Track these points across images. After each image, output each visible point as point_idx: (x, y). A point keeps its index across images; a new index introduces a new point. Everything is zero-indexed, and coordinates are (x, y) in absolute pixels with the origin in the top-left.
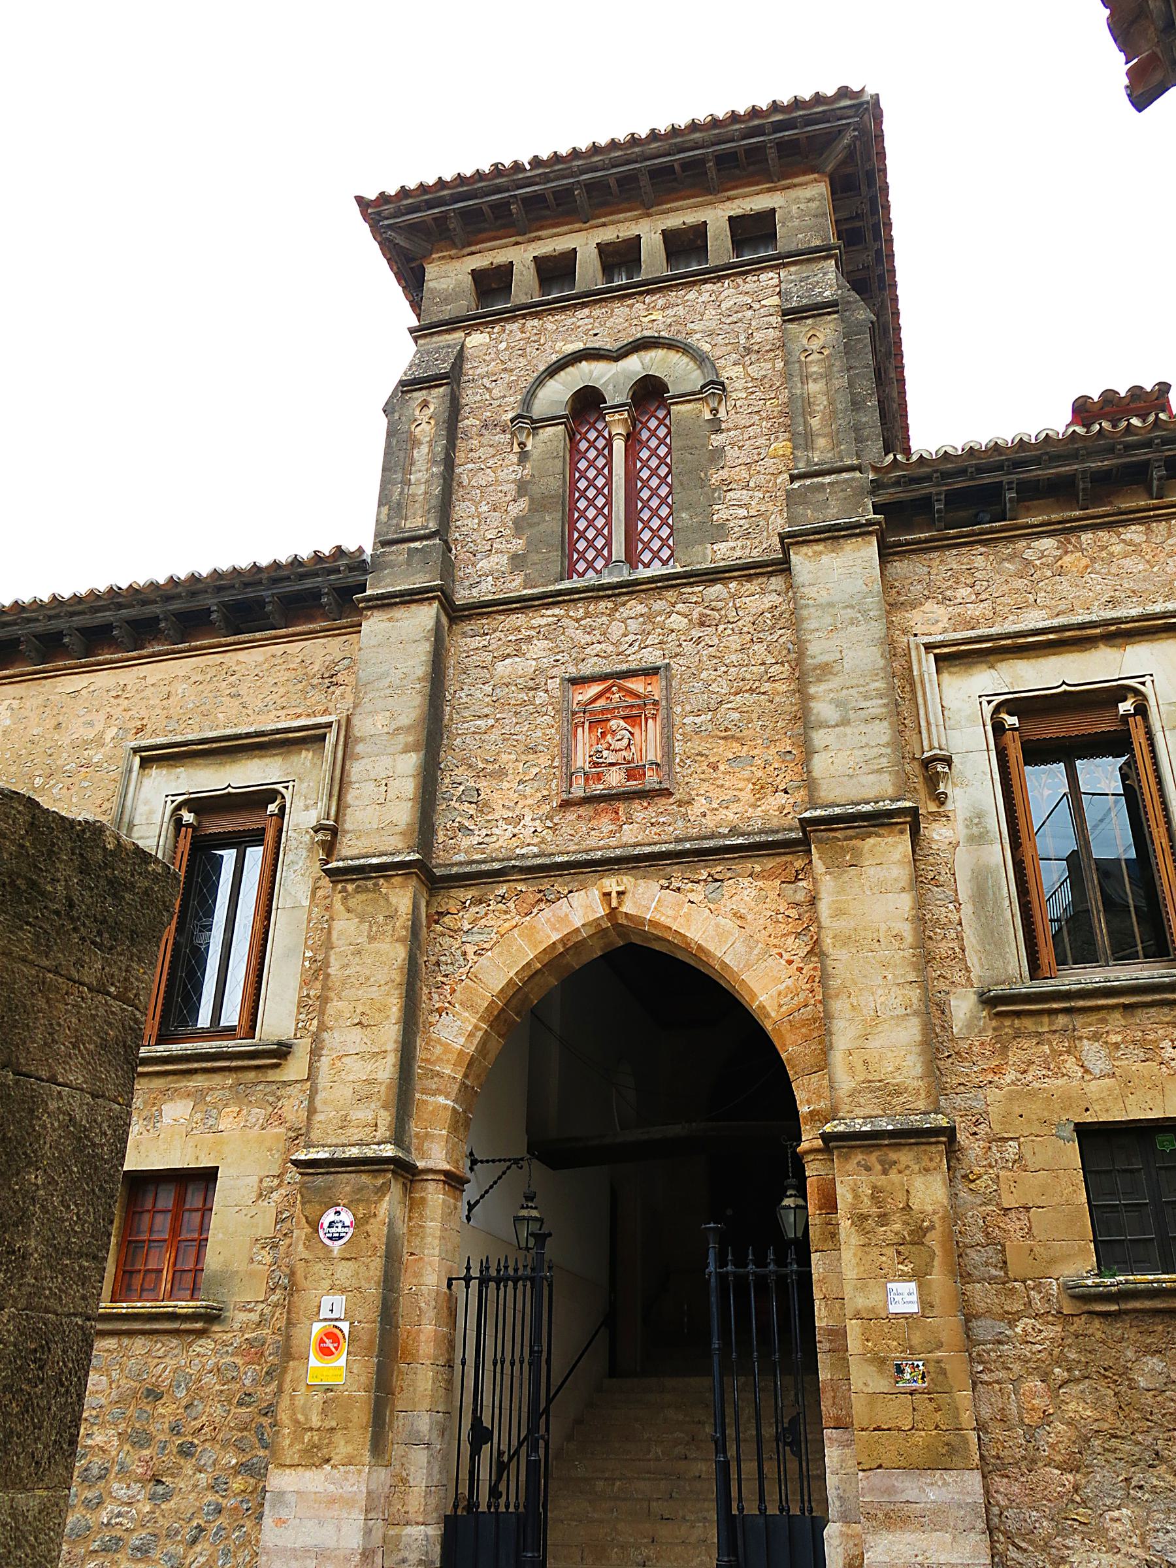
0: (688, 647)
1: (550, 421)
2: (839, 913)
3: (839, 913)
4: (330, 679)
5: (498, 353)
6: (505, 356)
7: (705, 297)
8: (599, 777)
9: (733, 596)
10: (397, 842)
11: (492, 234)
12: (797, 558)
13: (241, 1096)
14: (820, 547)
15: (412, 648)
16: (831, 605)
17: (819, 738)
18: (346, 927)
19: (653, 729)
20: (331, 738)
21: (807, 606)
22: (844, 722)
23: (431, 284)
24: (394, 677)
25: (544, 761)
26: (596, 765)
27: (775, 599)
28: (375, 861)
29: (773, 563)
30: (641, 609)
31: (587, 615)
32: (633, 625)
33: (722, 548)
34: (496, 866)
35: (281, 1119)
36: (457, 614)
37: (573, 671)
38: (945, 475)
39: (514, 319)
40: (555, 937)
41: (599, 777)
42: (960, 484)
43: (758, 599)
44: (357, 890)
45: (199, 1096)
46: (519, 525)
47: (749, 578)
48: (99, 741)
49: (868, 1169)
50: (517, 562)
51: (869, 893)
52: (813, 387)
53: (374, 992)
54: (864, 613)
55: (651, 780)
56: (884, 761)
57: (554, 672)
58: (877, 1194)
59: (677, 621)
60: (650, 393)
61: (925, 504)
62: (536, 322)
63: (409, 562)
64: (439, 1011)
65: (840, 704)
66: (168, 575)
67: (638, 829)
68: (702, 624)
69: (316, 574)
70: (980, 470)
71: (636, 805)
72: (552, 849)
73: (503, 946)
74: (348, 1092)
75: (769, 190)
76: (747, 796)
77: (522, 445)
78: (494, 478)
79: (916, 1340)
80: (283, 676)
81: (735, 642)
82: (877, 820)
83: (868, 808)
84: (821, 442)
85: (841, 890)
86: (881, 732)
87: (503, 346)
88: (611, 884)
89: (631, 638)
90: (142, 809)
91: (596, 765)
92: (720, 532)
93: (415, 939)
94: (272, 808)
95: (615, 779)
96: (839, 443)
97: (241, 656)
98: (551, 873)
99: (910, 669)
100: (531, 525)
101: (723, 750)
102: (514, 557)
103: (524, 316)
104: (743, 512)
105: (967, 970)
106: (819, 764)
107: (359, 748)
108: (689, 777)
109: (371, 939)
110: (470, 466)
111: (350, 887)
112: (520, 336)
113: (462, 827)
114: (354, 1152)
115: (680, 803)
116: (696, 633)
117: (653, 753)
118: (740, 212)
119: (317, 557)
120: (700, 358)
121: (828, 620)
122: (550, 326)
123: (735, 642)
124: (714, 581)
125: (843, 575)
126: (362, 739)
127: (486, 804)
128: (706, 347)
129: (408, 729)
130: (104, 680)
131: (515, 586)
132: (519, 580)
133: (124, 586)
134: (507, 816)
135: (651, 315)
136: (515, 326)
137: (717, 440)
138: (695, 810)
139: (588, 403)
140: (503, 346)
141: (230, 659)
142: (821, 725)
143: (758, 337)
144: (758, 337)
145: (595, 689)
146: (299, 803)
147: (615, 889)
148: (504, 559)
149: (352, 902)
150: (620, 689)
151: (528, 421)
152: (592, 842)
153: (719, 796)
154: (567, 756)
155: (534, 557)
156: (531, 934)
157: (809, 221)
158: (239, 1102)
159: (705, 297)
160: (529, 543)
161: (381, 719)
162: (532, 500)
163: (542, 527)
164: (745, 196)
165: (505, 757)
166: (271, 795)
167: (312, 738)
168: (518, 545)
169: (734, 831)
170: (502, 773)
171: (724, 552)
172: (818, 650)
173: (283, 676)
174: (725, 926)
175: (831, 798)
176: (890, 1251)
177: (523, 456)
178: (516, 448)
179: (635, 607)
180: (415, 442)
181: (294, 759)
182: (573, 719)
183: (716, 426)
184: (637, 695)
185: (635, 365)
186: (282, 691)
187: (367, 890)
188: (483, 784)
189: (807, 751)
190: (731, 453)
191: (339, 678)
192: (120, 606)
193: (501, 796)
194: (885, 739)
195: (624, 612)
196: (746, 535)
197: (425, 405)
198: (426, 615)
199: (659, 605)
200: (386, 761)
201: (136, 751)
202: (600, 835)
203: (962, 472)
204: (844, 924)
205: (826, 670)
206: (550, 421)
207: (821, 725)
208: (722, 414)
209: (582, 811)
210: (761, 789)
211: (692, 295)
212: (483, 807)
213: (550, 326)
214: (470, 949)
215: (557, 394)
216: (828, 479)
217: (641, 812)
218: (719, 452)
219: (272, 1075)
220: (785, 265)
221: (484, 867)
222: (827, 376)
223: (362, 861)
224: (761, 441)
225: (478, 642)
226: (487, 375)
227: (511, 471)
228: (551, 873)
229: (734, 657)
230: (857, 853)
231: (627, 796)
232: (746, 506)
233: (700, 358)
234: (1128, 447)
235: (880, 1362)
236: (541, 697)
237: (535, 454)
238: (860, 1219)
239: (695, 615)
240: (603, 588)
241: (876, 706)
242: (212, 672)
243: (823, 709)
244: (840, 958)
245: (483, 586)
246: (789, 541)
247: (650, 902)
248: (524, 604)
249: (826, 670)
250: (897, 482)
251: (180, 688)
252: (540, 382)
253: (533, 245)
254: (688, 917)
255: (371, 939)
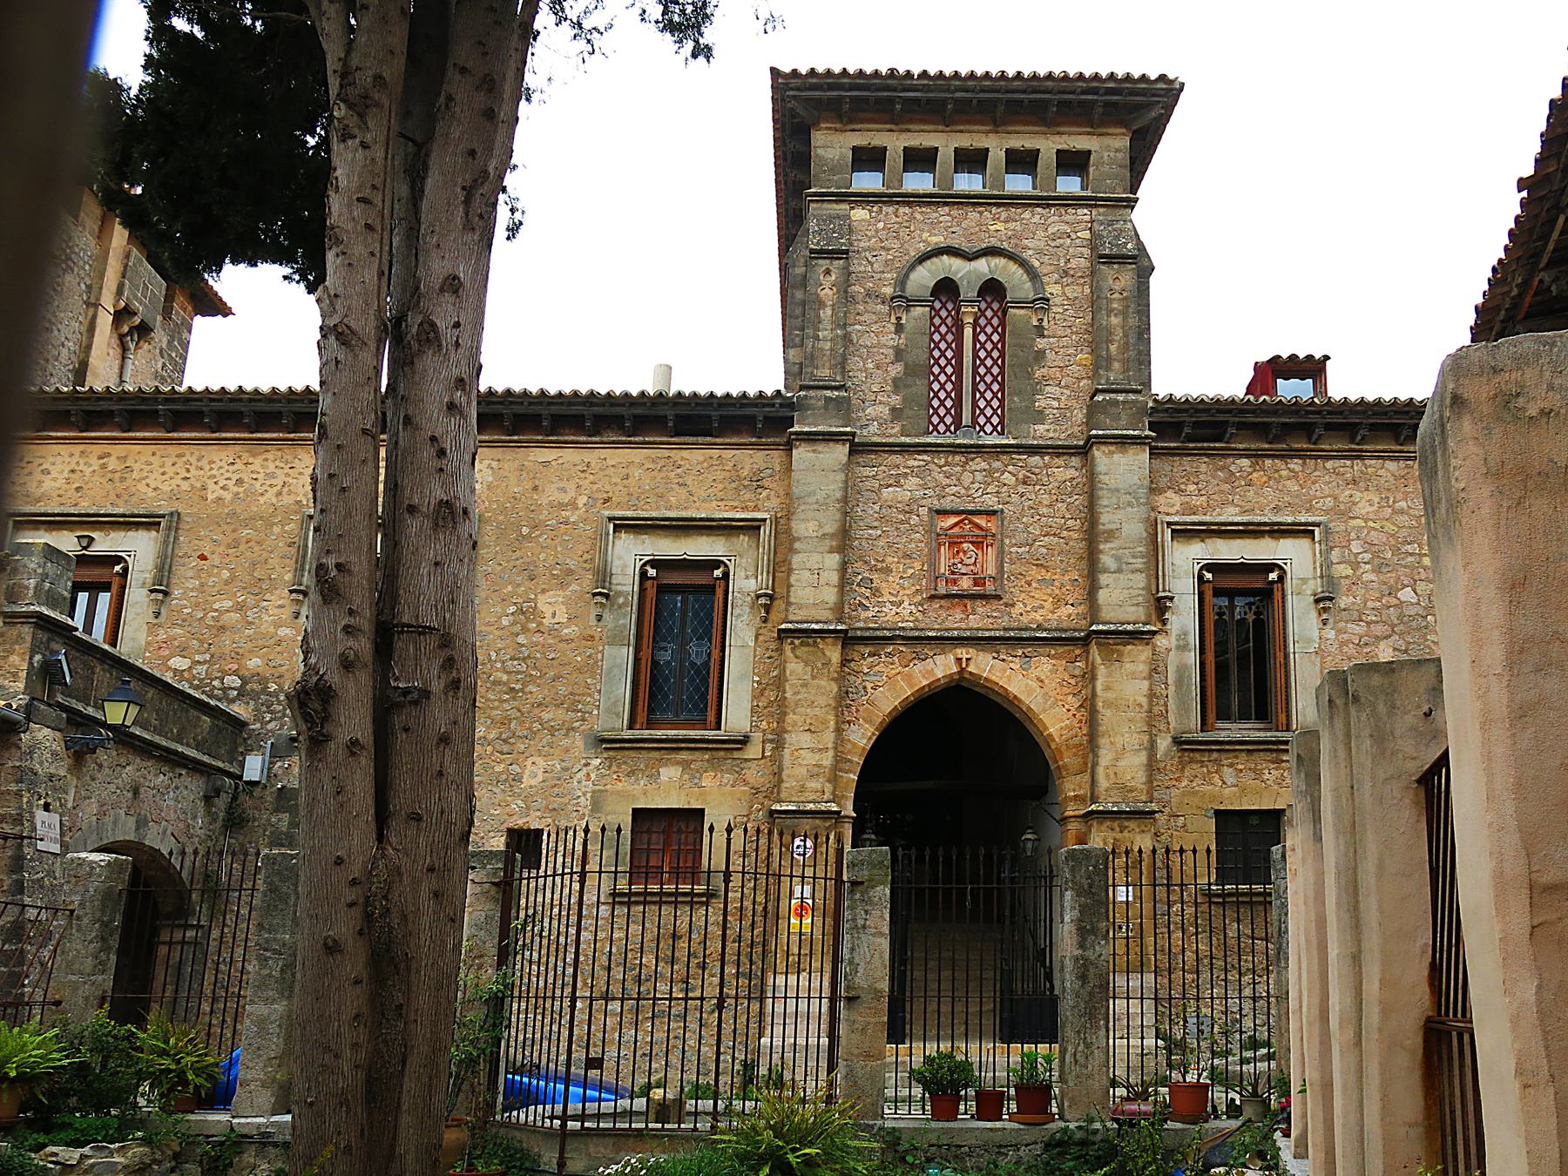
0: (1015, 498)
1: (920, 301)
2: (1107, 688)
3: (1107, 688)
4: (757, 483)
5: (877, 231)
6: (883, 234)
7: (1036, 219)
8: (955, 582)
9: (1047, 466)
10: (827, 615)
11: (870, 115)
12: (1098, 453)
13: (714, 765)
14: (1112, 448)
15: (832, 476)
16: (1117, 490)
17: (1104, 579)
18: (795, 668)
19: (991, 553)
20: (765, 531)
22: (1119, 571)
23: (820, 151)
24: (820, 496)
25: (917, 565)
26: (953, 573)
27: (1072, 473)
28: (814, 626)
29: (1076, 447)
30: (984, 465)
31: (947, 464)
32: (979, 477)
33: (1041, 428)
34: (888, 634)
35: (745, 782)
36: (859, 449)
37: (937, 505)
38: (1197, 411)
39: (891, 203)
40: (925, 682)
41: (955, 582)
42: (1204, 418)
43: (1065, 471)
44: (802, 644)
45: (686, 765)
46: (897, 384)
47: (1059, 455)
48: (573, 505)
50: (896, 413)
51: (1124, 682)
52: (1114, 320)
53: (817, 711)
54: (1137, 499)
55: (990, 588)
57: (924, 502)
59: (1007, 478)
60: (992, 289)
61: (1179, 426)
62: (907, 210)
63: (826, 408)
64: (849, 722)
65: (1118, 559)
66: (640, 389)
67: (979, 619)
68: (1025, 483)
69: (756, 405)
70: (1219, 411)
71: (978, 602)
72: (922, 626)
73: (893, 685)
74: (804, 771)
75: (1089, 133)
76: (1048, 605)
77: (899, 319)
78: (878, 341)
80: (720, 475)
81: (1046, 499)
82: (1135, 636)
83: (1130, 627)
84: (1116, 365)
85: (1109, 675)
86: (1140, 580)
87: (881, 225)
88: (963, 653)
89: (976, 486)
90: (617, 563)
91: (953, 573)
92: (1040, 417)
93: (841, 679)
94: (718, 573)
95: (965, 584)
96: (1128, 370)
97: (685, 454)
98: (920, 642)
100: (906, 386)
101: (1034, 573)
102: (893, 410)
103: (898, 203)
104: (1055, 404)
106: (1102, 595)
107: (797, 545)
108: (1013, 589)
109: (814, 678)
110: (858, 327)
111: (797, 642)
112: (895, 219)
113: (860, 604)
114: (811, 806)
115: (1006, 605)
116: (1021, 489)
117: (991, 570)
118: (1065, 147)
119: (761, 395)
120: (1033, 275)
121: (1114, 500)
122: (918, 216)
123: (1046, 499)
124: (1035, 453)
125: (1123, 469)
126: (799, 539)
127: (877, 590)
128: (1036, 264)
129: (832, 536)
130: (570, 456)
131: (894, 434)
132: (897, 429)
133: (603, 392)
134: (895, 603)
135: (997, 227)
136: (891, 209)
137: (1041, 343)
138: (1015, 611)
139: (946, 288)
140: (881, 225)
141: (677, 455)
142: (1106, 571)
143: (1073, 263)
144: (1073, 263)
145: (953, 520)
146: (741, 573)
147: (965, 656)
148: (887, 410)
149: (798, 652)
150: (971, 522)
151: (902, 300)
152: (948, 624)
153: (1031, 603)
154: (933, 563)
155: (910, 413)
156: (909, 678)
157: (1116, 169)
158: (714, 769)
159: (1036, 219)
160: (904, 400)
161: (812, 526)
162: (906, 366)
163: (914, 389)
164: (1070, 134)
165: (889, 559)
166: (716, 564)
167: (752, 527)
168: (896, 400)
169: (1040, 628)
170: (887, 571)
171: (1042, 432)
172: (1107, 519)
173: (720, 475)
174: (1034, 686)
175: (1108, 618)
177: (899, 328)
178: (893, 320)
179: (980, 464)
180: (822, 304)
181: (735, 540)
182: (938, 539)
183: (1040, 331)
184: (981, 529)
185: (982, 266)
186: (721, 486)
187: (808, 645)
188: (875, 576)
189: (1093, 589)
190: (1050, 355)
191: (765, 483)
192: (592, 404)
193: (888, 586)
194: (1142, 585)
195: (973, 465)
196: (1056, 421)
197: (828, 272)
198: (841, 452)
199: (997, 464)
200: (816, 557)
201: (610, 519)
202: (955, 620)
203: (1207, 411)
204: (1110, 695)
205: (1111, 535)
206: (920, 301)
207: (1106, 571)
208: (1045, 323)
209: (943, 602)
210: (1058, 602)
211: (1027, 215)
212: (876, 592)
213: (918, 216)
214: (869, 685)
215: (925, 277)
216: (1121, 397)
217: (981, 608)
218: (1040, 355)
219: (736, 755)
220: (1096, 206)
221: (879, 633)
222: (1124, 314)
223: (805, 626)
224: (1071, 351)
225: (867, 472)
226: (869, 249)
227: (890, 339)
228: (920, 642)
229: (1045, 510)
230: (1121, 654)
231: (973, 597)
232: (1058, 399)
233: (1033, 275)
234: (1308, 412)
236: (914, 520)
237: (908, 327)
239: (1021, 476)
240: (960, 446)
241: (1139, 563)
242: (662, 462)
243: (1107, 560)
244: (1106, 716)
245: (871, 428)
247: (985, 666)
248: (904, 449)
249: (1111, 535)
250: (1166, 410)
251: (637, 473)
252: (912, 267)
253: (904, 136)
254: (1009, 678)
255: (814, 678)
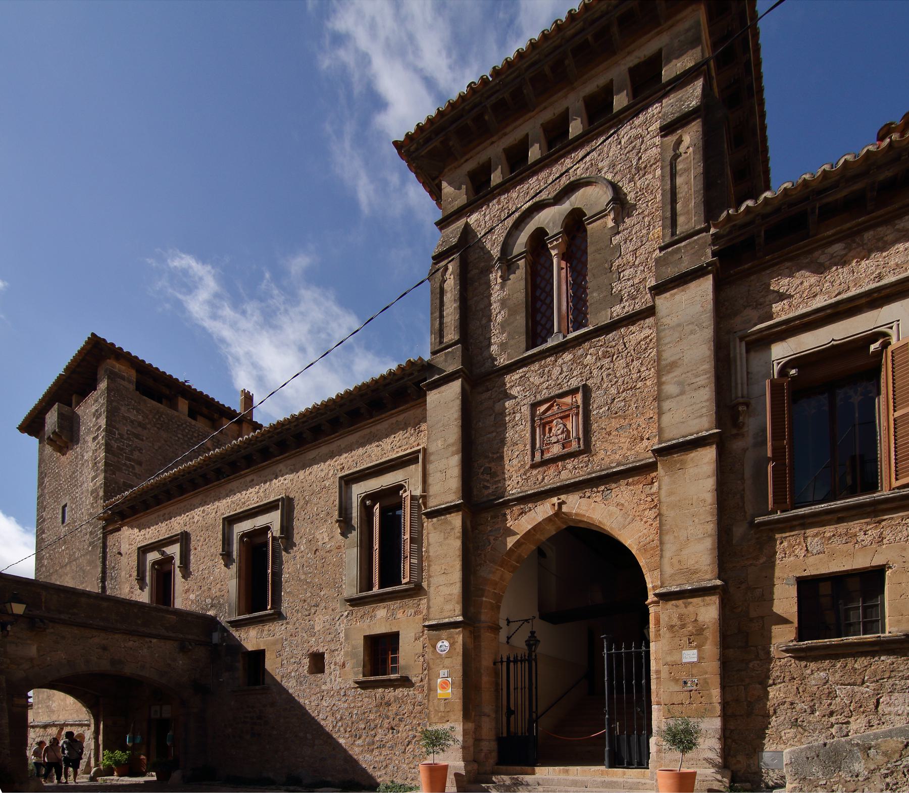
21: (664, 330)
49: (677, 606)
56: (704, 410)
58: (681, 617)
79: (694, 671)
99: (729, 354)
105: (745, 512)
176: (686, 639)
235: (676, 681)
238: (671, 628)
246: (658, 290)
249: (673, 365)
